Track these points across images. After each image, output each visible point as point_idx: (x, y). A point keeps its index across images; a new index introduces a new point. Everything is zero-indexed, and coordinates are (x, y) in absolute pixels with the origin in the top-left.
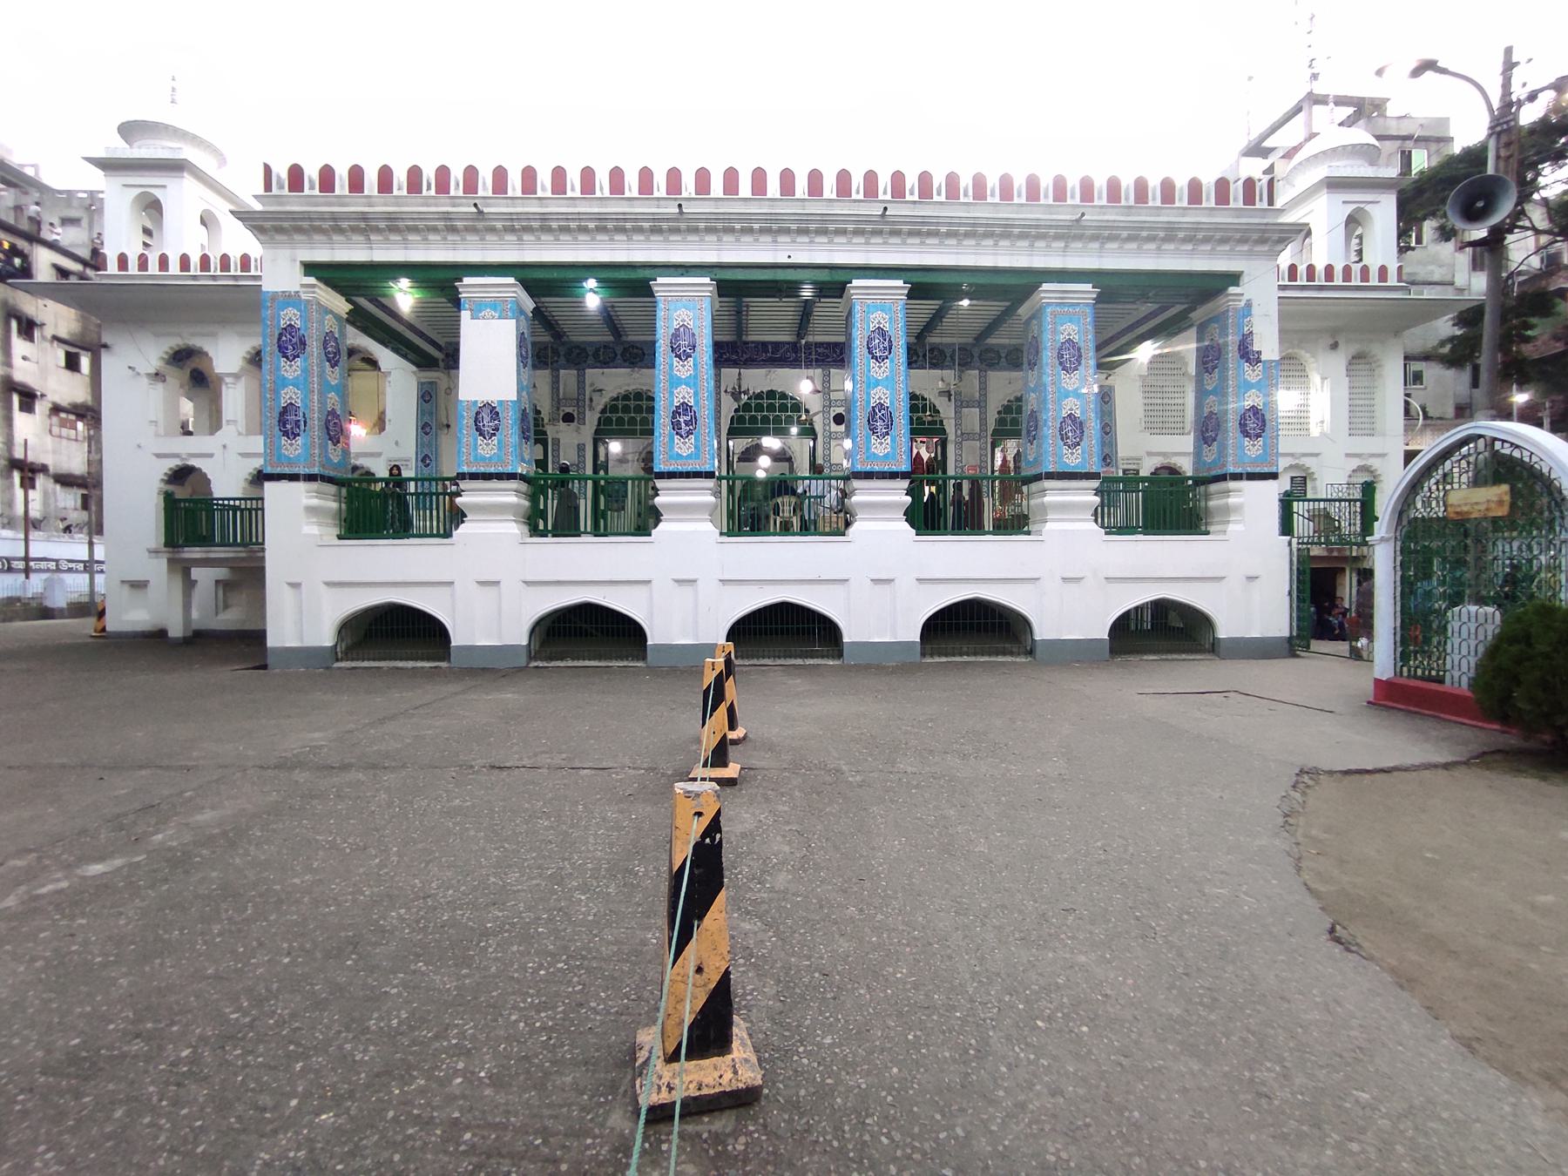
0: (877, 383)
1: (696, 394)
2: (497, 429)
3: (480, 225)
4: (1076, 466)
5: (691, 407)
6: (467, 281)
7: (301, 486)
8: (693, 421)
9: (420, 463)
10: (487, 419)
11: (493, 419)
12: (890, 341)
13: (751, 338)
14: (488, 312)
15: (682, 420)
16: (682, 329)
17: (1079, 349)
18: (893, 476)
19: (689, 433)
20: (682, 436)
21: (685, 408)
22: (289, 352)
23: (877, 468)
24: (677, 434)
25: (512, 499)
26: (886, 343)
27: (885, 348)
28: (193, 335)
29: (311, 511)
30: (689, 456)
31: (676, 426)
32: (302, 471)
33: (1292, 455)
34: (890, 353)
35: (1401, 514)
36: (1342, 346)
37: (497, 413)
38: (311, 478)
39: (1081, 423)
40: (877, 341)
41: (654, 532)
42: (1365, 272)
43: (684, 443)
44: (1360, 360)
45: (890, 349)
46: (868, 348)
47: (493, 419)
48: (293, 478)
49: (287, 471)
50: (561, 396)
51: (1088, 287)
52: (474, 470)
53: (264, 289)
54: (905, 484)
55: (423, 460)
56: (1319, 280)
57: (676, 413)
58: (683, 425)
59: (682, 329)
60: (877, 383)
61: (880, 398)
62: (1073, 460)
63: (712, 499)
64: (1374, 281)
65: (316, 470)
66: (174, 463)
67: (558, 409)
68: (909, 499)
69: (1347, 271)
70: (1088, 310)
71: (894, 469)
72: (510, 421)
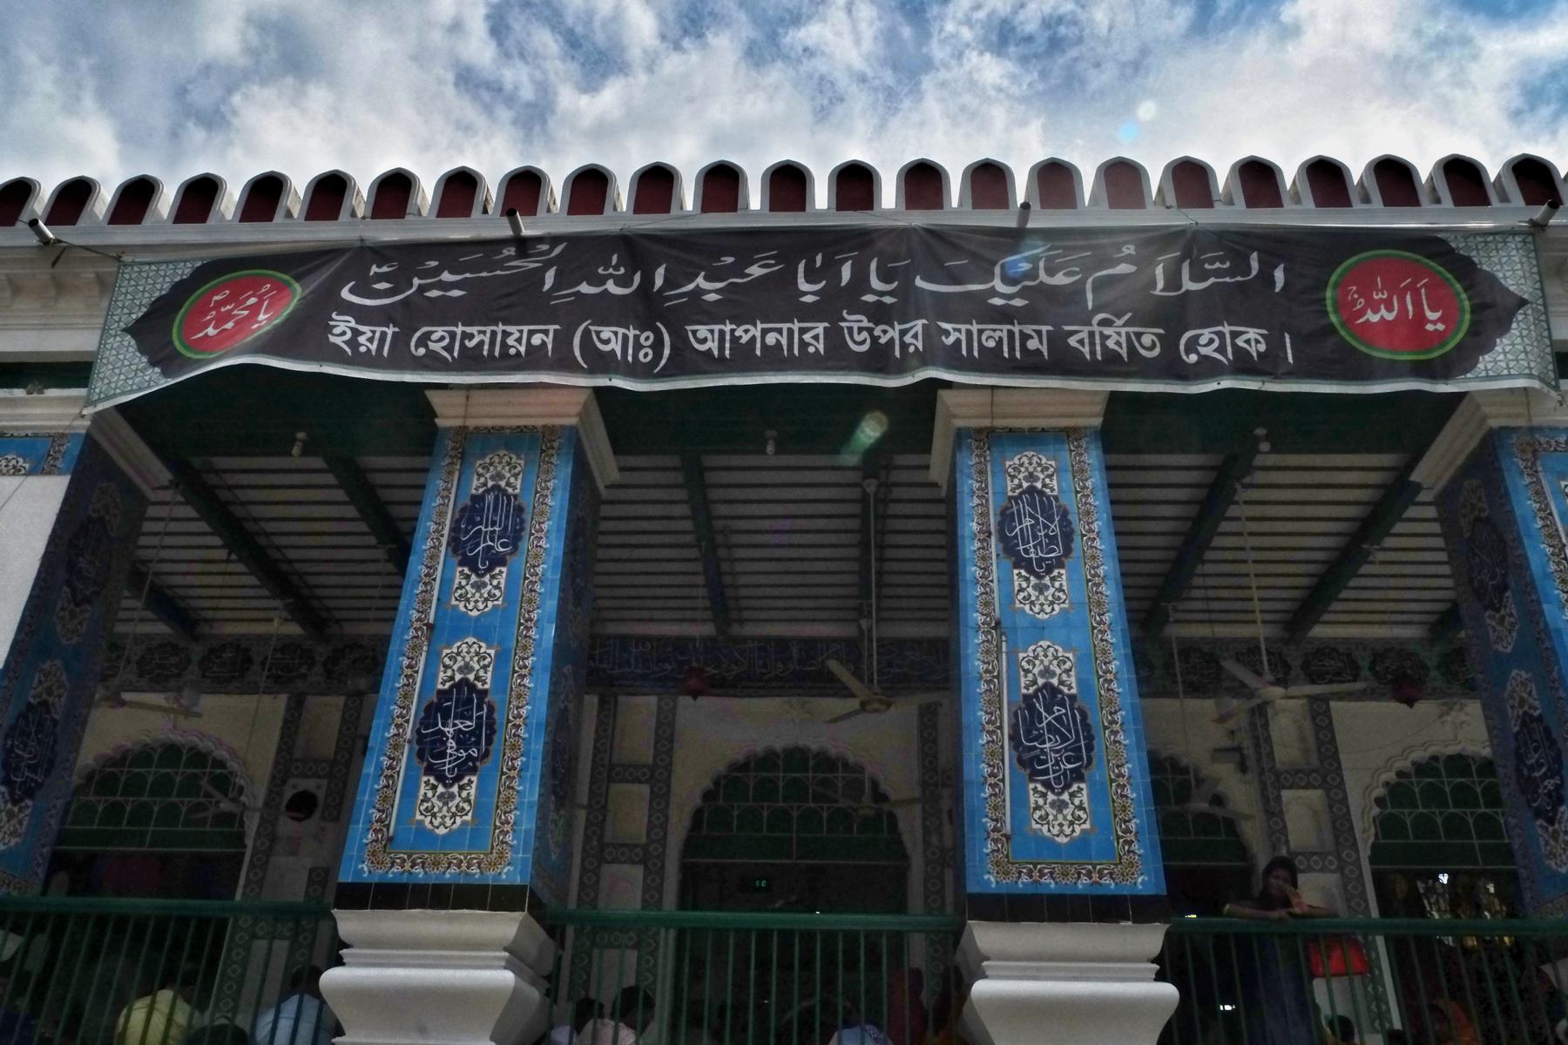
0: (1039, 630)
1: (501, 657)
5: (483, 694)
8: (482, 736)
12: (1065, 523)
13: (750, 630)
15: (449, 730)
16: (490, 498)
19: (466, 768)
20: (441, 778)
21: (464, 696)
23: (1050, 885)
24: (430, 770)
26: (1055, 527)
27: (1052, 539)
31: (428, 748)
34: (1068, 551)
40: (1028, 522)
43: (446, 798)
45: (1068, 536)
46: (1002, 538)
50: (298, 754)
54: (1152, 938)
57: (435, 710)
58: (452, 743)
59: (490, 498)
60: (1039, 630)
61: (1046, 672)
63: (507, 977)
67: (284, 782)
68: (1169, 990)
71: (1110, 885)
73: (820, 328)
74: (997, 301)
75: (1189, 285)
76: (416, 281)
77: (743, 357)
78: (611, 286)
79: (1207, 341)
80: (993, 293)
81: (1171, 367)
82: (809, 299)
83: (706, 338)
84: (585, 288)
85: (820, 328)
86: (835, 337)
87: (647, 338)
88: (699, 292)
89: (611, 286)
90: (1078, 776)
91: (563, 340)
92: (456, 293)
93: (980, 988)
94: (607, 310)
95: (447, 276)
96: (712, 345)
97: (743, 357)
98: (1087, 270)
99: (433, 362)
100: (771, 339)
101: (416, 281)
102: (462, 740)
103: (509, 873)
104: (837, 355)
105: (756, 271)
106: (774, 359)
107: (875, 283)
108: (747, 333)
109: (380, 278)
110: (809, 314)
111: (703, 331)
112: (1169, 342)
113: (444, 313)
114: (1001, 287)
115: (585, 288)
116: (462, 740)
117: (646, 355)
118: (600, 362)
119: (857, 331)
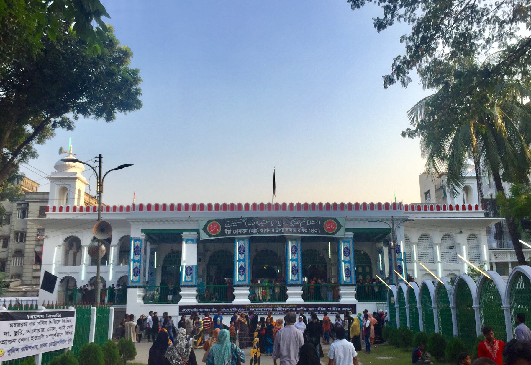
3: (189, 220)
4: (349, 283)
6: (185, 233)
7: (138, 289)
9: (150, 275)
10: (189, 271)
11: (190, 271)
14: (190, 242)
18: (298, 285)
19: (243, 274)
22: (137, 253)
26: (296, 249)
28: (76, 232)
29: (139, 296)
30: (243, 281)
32: (138, 284)
35: (512, 290)
36: (464, 231)
37: (191, 269)
38: (140, 287)
39: (350, 270)
41: (233, 301)
42: (470, 207)
44: (472, 236)
47: (190, 271)
48: (136, 287)
53: (131, 236)
54: (302, 288)
55: (151, 274)
62: (348, 280)
66: (64, 275)
68: (302, 292)
69: (464, 207)
70: (351, 239)
73: (273, 229)
74: (291, 226)
75: (310, 224)
76: (232, 224)
77: (266, 233)
79: (312, 230)
81: (308, 233)
82: (272, 226)
83: (262, 230)
84: (250, 224)
85: (273, 229)
86: (275, 230)
87: (256, 230)
88: (261, 225)
90: (296, 274)
91: (248, 231)
92: (236, 225)
93: (287, 292)
94: (252, 227)
95: (235, 223)
96: (263, 231)
97: (266, 233)
98: (300, 222)
99: (235, 234)
100: (269, 231)
101: (232, 224)
102: (242, 272)
104: (275, 233)
105: (267, 222)
106: (269, 233)
107: (279, 224)
108: (266, 230)
109: (228, 223)
110: (272, 227)
111: (262, 229)
112: (308, 230)
113: (236, 228)
114: (291, 223)
115: (250, 224)
116: (242, 272)
117: (256, 232)
118: (252, 233)
119: (278, 230)
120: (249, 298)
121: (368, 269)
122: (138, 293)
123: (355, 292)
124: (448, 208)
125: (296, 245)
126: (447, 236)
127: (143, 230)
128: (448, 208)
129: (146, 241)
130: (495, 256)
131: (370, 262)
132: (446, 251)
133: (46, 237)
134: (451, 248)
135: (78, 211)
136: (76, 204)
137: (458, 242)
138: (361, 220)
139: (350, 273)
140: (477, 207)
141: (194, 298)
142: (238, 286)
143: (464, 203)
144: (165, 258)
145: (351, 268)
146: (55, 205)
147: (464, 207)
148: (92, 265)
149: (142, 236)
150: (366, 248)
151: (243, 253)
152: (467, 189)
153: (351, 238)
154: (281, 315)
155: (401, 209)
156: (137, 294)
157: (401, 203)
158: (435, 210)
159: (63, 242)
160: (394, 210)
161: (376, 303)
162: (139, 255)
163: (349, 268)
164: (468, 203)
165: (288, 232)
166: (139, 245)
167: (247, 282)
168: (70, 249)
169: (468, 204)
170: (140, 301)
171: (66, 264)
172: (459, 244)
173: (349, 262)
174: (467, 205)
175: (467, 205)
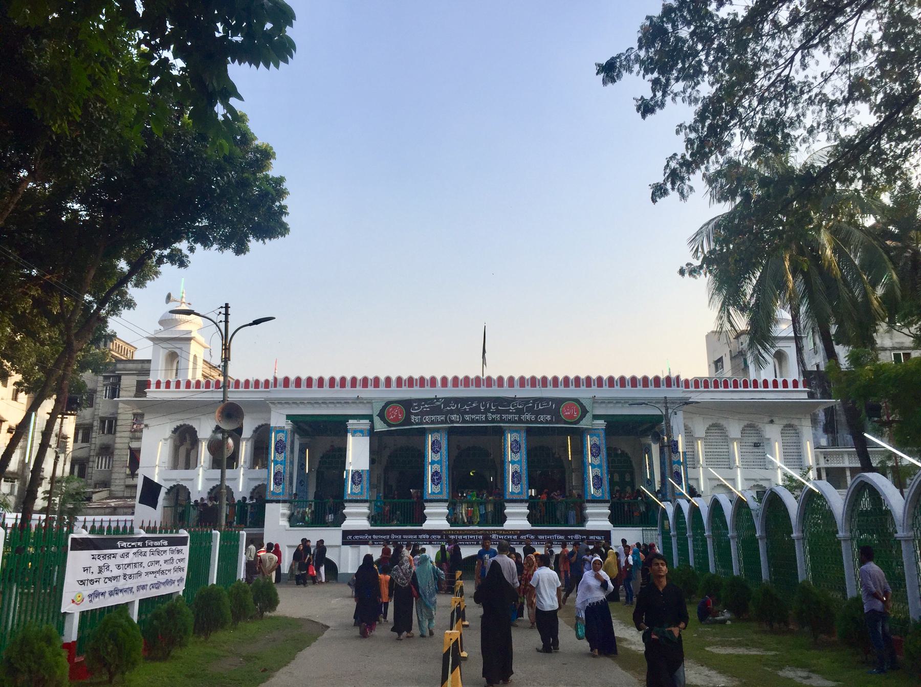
2: (361, 482)
3: (358, 401)
6: (351, 421)
7: (281, 505)
8: (440, 478)
10: (357, 477)
17: (599, 447)
18: (521, 501)
19: (438, 483)
25: (366, 511)
29: (283, 515)
30: (438, 493)
32: (281, 498)
33: (754, 480)
35: (853, 511)
36: (776, 419)
38: (284, 502)
42: (785, 384)
44: (789, 428)
48: (278, 502)
49: (275, 498)
51: (602, 422)
52: (351, 498)
53: (271, 425)
54: (527, 505)
55: (300, 482)
56: (761, 387)
62: (599, 494)
64: (791, 388)
65: (287, 498)
66: (172, 484)
69: (775, 383)
70: (603, 431)
72: (365, 477)
75: (540, 407)
77: (473, 421)
78: (452, 407)
79: (542, 418)
80: (510, 409)
81: (536, 422)
83: (467, 417)
84: (448, 408)
86: (486, 417)
88: (465, 409)
89: (452, 407)
90: (519, 484)
91: (446, 418)
93: (505, 511)
94: (452, 412)
95: (426, 406)
96: (468, 419)
97: (473, 421)
99: (427, 423)
103: (445, 498)
104: (487, 421)
105: (474, 405)
106: (477, 421)
107: (493, 408)
108: (473, 417)
109: (416, 406)
110: (483, 413)
111: (466, 416)
112: (536, 418)
113: (427, 413)
114: (511, 407)
115: (448, 408)
116: (437, 479)
118: (452, 422)
120: (448, 520)
121: (628, 479)
122: (281, 511)
123: (610, 511)
124: (750, 385)
125: (518, 439)
126: (750, 428)
127: (289, 417)
128: (750, 385)
129: (293, 432)
130: (825, 458)
131: (632, 466)
132: (748, 451)
133: (146, 426)
134: (756, 445)
135: (193, 387)
136: (190, 378)
137: (767, 437)
138: (617, 403)
139: (602, 483)
140: (795, 383)
141: (365, 518)
142: (431, 501)
143: (776, 377)
144: (322, 458)
145: (602, 474)
146: (159, 378)
147: (775, 383)
148: (213, 468)
149: (288, 425)
150: (624, 445)
151: (438, 452)
152: (780, 356)
153: (602, 429)
154: (466, 546)
155: (678, 386)
156: (279, 512)
157: (678, 378)
158: (731, 387)
159: (170, 433)
160: (632, 387)
161: (641, 528)
162: (283, 454)
163: (600, 475)
164: (781, 377)
165: (428, 422)
166: (284, 439)
167: (445, 496)
168: (182, 444)
169: (783, 379)
170: (284, 523)
171: (175, 466)
172: (769, 439)
173: (600, 466)
174: (780, 380)
175: (780, 380)
